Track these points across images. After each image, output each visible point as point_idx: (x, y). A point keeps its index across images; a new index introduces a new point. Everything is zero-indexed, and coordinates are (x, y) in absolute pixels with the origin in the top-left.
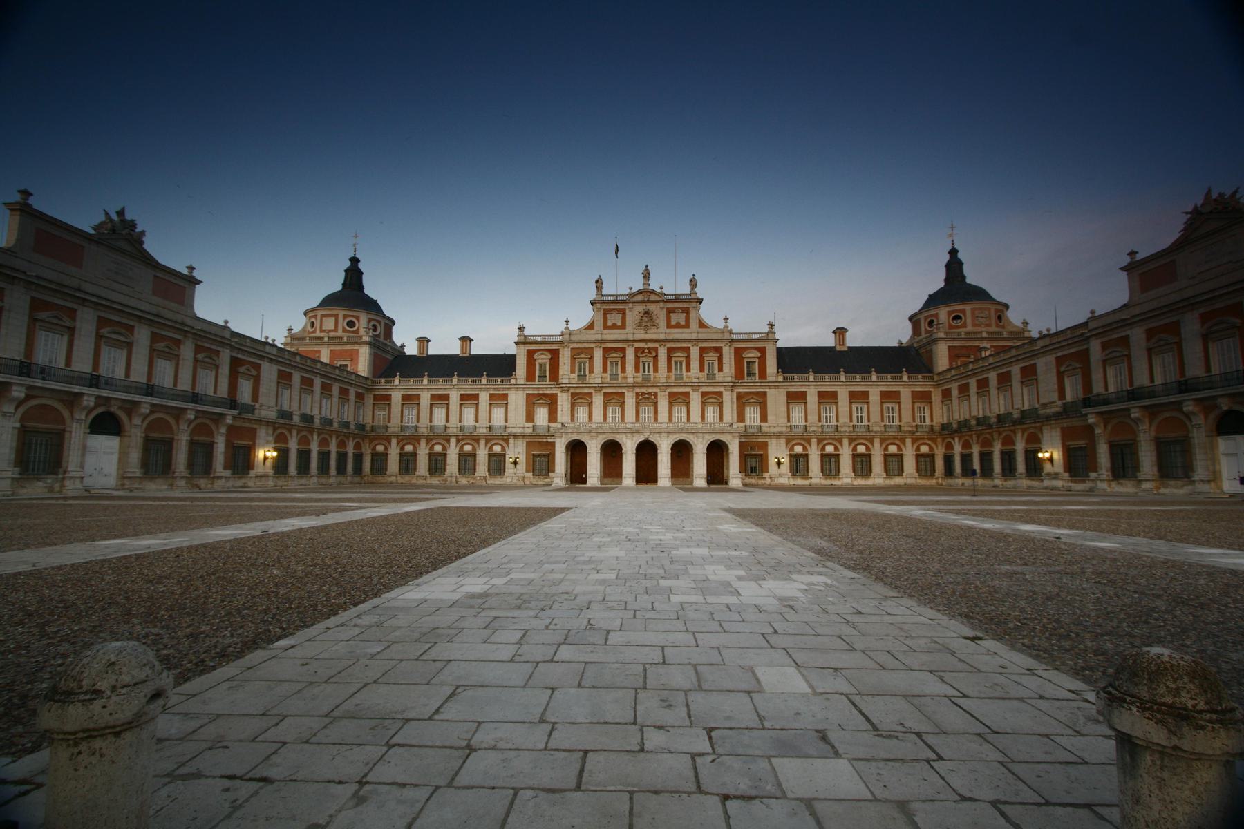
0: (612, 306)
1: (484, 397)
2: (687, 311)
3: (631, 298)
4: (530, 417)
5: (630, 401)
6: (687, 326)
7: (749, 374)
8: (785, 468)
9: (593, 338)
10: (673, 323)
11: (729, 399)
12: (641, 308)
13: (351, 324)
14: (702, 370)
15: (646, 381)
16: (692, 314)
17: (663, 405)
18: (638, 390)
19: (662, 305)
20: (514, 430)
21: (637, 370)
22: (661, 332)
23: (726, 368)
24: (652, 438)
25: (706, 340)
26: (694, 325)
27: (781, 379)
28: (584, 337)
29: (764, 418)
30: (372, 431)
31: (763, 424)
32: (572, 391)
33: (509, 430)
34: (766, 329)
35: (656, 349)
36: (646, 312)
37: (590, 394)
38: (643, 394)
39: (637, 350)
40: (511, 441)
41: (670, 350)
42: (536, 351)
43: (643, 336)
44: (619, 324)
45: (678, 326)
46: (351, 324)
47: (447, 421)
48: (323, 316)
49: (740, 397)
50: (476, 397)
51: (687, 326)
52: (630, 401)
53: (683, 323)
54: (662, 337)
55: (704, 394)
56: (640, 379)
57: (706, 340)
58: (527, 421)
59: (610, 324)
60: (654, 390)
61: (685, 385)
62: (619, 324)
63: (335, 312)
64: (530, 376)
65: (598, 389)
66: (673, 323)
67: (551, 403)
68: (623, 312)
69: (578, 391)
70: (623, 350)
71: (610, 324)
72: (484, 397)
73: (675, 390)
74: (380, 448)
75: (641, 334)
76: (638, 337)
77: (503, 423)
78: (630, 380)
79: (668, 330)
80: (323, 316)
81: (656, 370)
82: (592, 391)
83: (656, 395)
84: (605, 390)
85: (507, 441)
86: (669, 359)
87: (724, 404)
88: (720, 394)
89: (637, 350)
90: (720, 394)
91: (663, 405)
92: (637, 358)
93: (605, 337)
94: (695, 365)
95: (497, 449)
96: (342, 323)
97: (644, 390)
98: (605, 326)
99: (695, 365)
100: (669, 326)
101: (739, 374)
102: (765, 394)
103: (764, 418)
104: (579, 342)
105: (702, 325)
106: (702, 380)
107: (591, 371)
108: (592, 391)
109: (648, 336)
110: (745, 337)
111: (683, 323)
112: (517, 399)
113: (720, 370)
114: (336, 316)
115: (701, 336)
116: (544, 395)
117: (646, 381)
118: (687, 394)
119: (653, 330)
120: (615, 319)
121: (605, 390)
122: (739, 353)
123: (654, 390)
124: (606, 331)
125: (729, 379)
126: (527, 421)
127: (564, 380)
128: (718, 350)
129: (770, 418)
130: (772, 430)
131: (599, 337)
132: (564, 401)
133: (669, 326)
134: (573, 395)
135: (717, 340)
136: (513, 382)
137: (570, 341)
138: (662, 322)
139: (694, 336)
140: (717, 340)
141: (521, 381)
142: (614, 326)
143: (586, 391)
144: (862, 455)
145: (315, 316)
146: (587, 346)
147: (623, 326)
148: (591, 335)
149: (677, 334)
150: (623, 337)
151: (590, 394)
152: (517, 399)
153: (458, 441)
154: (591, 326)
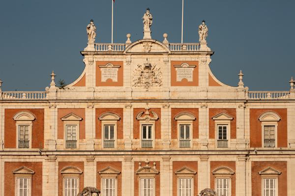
5: (128, 171)
6: (195, 83)
9: (85, 96)
10: (179, 79)
11: (244, 170)
12: (142, 61)
14: (212, 136)
15: (147, 149)
17: (166, 175)
19: (165, 57)
21: (136, 136)
22: (163, 90)
23: (239, 133)
25: (217, 101)
32: (60, 159)
35: (158, 111)
36: (148, 67)
37: (81, 164)
38: (143, 163)
39: (136, 110)
41: (175, 112)
44: (115, 80)
45: (184, 83)
49: (256, 167)
52: (128, 171)
53: (190, 80)
54: (165, 96)
55: (213, 164)
56: (139, 146)
57: (217, 101)
59: (104, 80)
60: (156, 159)
61: (193, 152)
62: (115, 80)
65: (92, 155)
66: (179, 79)
67: (35, 172)
68: (120, 66)
69: (67, 159)
70: (120, 111)
71: (104, 80)
75: (140, 93)
76: (137, 95)
78: (128, 147)
79: (173, 88)
81: (158, 136)
82: (83, 159)
83: (158, 164)
84: (98, 159)
86: (174, 122)
87: (237, 176)
88: (232, 164)
89: (136, 110)
90: (232, 164)
91: (166, 175)
92: (136, 120)
93: (98, 95)
94: (204, 129)
97: (144, 159)
99: (204, 129)
100: (174, 83)
102: (284, 164)
106: (211, 147)
107: (82, 136)
108: (83, 159)
109: (149, 96)
111: (190, 80)
113: (234, 136)
115: (211, 96)
116: (26, 164)
117: (147, 149)
118: (194, 164)
119: (155, 87)
120: (110, 74)
121: (98, 159)
123: (156, 159)
125: (243, 147)
127: (49, 146)
128: (231, 112)
131: (91, 95)
132: (49, 171)
133: (174, 83)
134: (61, 164)
135: (229, 101)
137: (57, 100)
138: (166, 78)
139: (202, 96)
140: (229, 101)
142: (109, 83)
143: (76, 159)
147: (120, 83)
151: (81, 164)
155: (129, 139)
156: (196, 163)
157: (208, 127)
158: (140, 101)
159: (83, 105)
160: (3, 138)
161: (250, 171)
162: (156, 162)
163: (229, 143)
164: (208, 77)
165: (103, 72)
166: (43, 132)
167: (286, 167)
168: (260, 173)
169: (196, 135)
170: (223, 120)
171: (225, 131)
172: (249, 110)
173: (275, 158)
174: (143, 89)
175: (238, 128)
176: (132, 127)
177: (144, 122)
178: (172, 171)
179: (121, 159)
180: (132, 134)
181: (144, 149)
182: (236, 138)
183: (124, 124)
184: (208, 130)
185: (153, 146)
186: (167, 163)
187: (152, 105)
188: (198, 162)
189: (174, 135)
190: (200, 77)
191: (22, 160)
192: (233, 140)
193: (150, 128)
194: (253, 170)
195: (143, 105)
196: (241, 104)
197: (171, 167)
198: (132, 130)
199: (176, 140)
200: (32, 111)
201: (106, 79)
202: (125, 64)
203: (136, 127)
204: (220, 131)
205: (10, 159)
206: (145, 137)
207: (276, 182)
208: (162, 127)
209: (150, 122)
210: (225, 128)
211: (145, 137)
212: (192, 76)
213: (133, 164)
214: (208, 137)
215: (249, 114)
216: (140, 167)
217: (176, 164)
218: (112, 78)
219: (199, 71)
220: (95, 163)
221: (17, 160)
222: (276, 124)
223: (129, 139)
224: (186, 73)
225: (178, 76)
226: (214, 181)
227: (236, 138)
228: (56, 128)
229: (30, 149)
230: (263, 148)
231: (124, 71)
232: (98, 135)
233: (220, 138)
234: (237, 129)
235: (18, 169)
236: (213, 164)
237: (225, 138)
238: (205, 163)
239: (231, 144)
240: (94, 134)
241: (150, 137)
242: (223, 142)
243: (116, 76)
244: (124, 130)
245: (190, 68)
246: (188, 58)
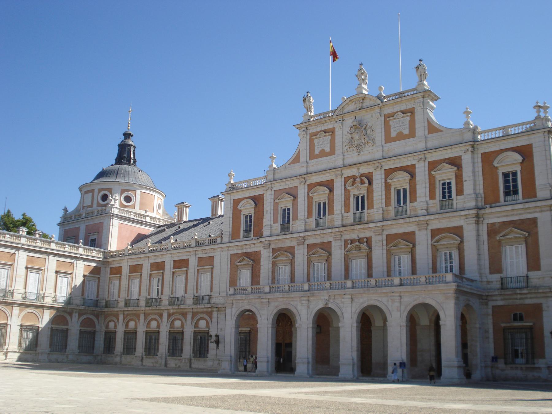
3: (339, 114)
14: (432, 196)
16: (419, 117)
21: (347, 210)
23: (468, 187)
26: (421, 130)
29: (534, 262)
31: (531, 274)
32: (273, 246)
33: (213, 301)
40: (215, 314)
44: (328, 149)
47: (211, 291)
51: (412, 134)
53: (406, 132)
75: (353, 157)
76: (348, 161)
77: (208, 292)
83: (368, 241)
85: (210, 314)
86: (388, 187)
94: (422, 190)
95: (202, 324)
99: (422, 190)
100: (388, 139)
101: (490, 200)
102: (534, 221)
103: (534, 262)
105: (432, 128)
108: (294, 243)
111: (406, 132)
113: (460, 192)
121: (307, 242)
129: (544, 262)
133: (388, 139)
134: (274, 251)
138: (379, 135)
147: (332, 152)
148: (299, 169)
149: (397, 147)
153: (169, 315)
154: (296, 159)
155: (339, 213)
156: (413, 233)
157: (428, 185)
160: (231, 230)
161: (485, 237)
162: (367, 238)
163: (455, 202)
164: (426, 124)
165: (316, 144)
166: (263, 219)
167: (536, 226)
168: (498, 238)
170: (446, 174)
171: (450, 188)
172: (480, 156)
173: (520, 214)
175: (466, 181)
176: (343, 199)
178: (385, 247)
180: (343, 208)
181: (355, 223)
182: (463, 195)
183: (335, 197)
184: (428, 190)
185: (366, 219)
186: (379, 238)
188: (416, 232)
190: (417, 126)
192: (459, 197)
194: (489, 235)
196: (467, 147)
197: (385, 243)
198: (343, 203)
199: (390, 208)
201: (319, 150)
202: (336, 130)
203: (347, 198)
204: (444, 189)
206: (357, 209)
208: (375, 194)
210: (449, 183)
211: (357, 209)
212: (408, 126)
213: (343, 243)
214: (428, 199)
215: (480, 160)
216: (349, 246)
218: (324, 148)
219: (416, 118)
220: (306, 246)
221: (240, 252)
222: (518, 169)
224: (401, 124)
225: (392, 130)
226: (436, 256)
227: (463, 195)
228: (272, 212)
231: (336, 138)
233: (444, 197)
234: (464, 183)
235: (239, 260)
236: (435, 233)
237: (450, 196)
238: (424, 232)
239: (457, 201)
240: (306, 214)
242: (447, 203)
243: (329, 145)
244: (335, 205)
245: (405, 118)
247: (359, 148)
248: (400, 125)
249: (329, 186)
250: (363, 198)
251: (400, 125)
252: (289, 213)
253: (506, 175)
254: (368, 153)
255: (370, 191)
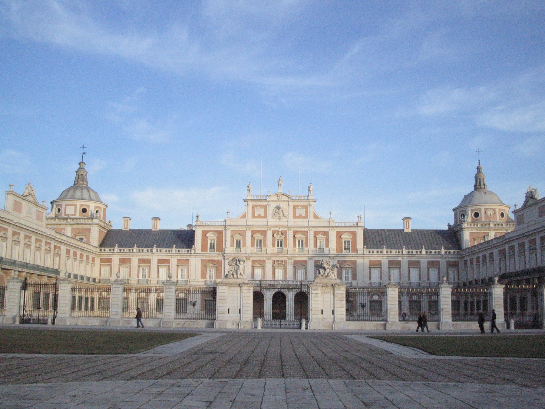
0: (258, 203)
1: (174, 261)
2: (306, 207)
4: (204, 275)
5: (269, 265)
6: (306, 217)
7: (345, 249)
8: (367, 309)
13: (84, 211)
18: (274, 259)
20: (193, 283)
21: (274, 245)
24: (284, 291)
27: (365, 252)
28: (239, 223)
30: (99, 282)
31: (353, 281)
34: (356, 220)
42: (208, 232)
43: (278, 223)
44: (262, 215)
46: (84, 211)
48: (66, 205)
50: (168, 261)
53: (304, 215)
58: (202, 277)
59: (256, 215)
62: (262, 215)
63: (74, 202)
64: (204, 248)
68: (265, 207)
71: (256, 215)
72: (174, 261)
73: (298, 259)
74: (105, 294)
80: (66, 205)
96: (79, 210)
97: (277, 259)
98: (253, 216)
104: (236, 226)
110: (343, 225)
111: (304, 215)
112: (195, 263)
114: (75, 205)
119: (284, 219)
121: (252, 258)
122: (339, 235)
124: (254, 219)
126: (202, 277)
130: (360, 285)
133: (295, 217)
136: (193, 251)
141: (200, 252)
142: (259, 217)
144: (415, 302)
145: (61, 205)
146: (241, 229)
147: (265, 216)
148: (243, 222)
150: (265, 224)
152: (195, 263)
158: (276, 226)
159: (244, 229)
169: (307, 246)
174: (277, 220)
177: (278, 238)
179: (265, 259)
187: (281, 229)
189: (295, 245)
191: (211, 259)
193: (281, 242)
195: (277, 229)
200: (217, 232)
203: (274, 241)
205: (204, 259)
206: (278, 246)
207: (350, 272)
209: (281, 238)
217: (296, 262)
221: (208, 259)
223: (270, 248)
229: (215, 252)
230: (343, 253)
232: (253, 245)
241: (281, 246)
246: (302, 203)
247: (279, 218)
248: (301, 211)
249: (264, 233)
250: (281, 242)
251: (301, 211)
252: (240, 243)
253: (345, 242)
254: (283, 222)
255: (286, 238)
